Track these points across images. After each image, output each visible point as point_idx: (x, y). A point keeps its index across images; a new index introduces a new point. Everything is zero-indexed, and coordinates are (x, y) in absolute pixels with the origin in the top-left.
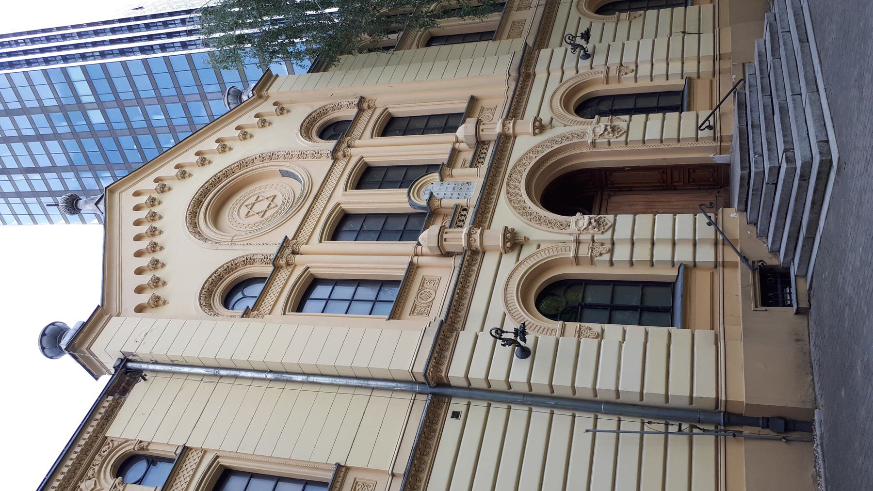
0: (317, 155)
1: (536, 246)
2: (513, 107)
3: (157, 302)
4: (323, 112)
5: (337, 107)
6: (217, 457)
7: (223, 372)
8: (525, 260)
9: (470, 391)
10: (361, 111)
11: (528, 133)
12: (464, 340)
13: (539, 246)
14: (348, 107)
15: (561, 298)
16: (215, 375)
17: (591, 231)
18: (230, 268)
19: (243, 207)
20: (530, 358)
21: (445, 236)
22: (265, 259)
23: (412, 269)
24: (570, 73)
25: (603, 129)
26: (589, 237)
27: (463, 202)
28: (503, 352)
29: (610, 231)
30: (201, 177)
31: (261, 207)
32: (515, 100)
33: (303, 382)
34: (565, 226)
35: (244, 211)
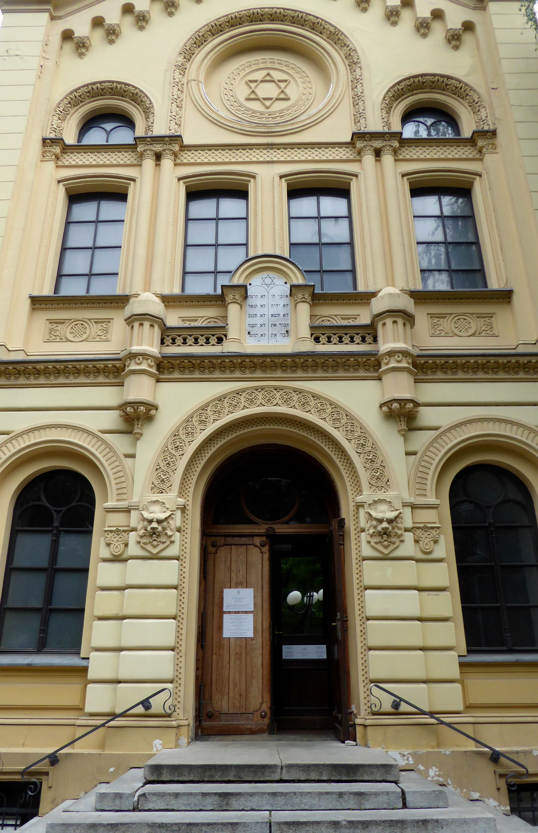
0: (358, 116)
1: (130, 451)
2: (501, 360)
4: (460, 90)
5: (475, 106)
18: (136, 97)
19: (265, 72)
22: (149, 128)
25: (380, 516)
26: (133, 524)
27: (232, 333)
34: (160, 485)
35: (259, 75)
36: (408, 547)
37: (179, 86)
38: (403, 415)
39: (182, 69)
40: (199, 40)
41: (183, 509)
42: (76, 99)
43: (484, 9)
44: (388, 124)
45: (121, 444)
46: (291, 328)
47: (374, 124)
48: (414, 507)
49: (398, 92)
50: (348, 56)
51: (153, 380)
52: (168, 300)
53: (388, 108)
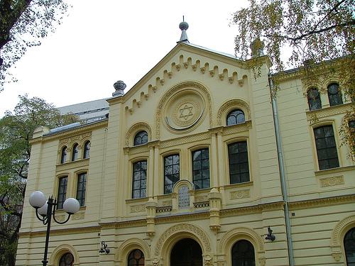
0: (211, 122)
4: (243, 104)
5: (248, 109)
12: (113, 231)
18: (147, 126)
24: (260, 232)
31: (186, 112)
35: (183, 107)
37: (158, 120)
38: (216, 230)
39: (159, 113)
40: (163, 101)
41: (162, 259)
42: (130, 131)
44: (220, 123)
48: (218, 256)
49: (222, 109)
52: (159, 197)
53: (219, 116)
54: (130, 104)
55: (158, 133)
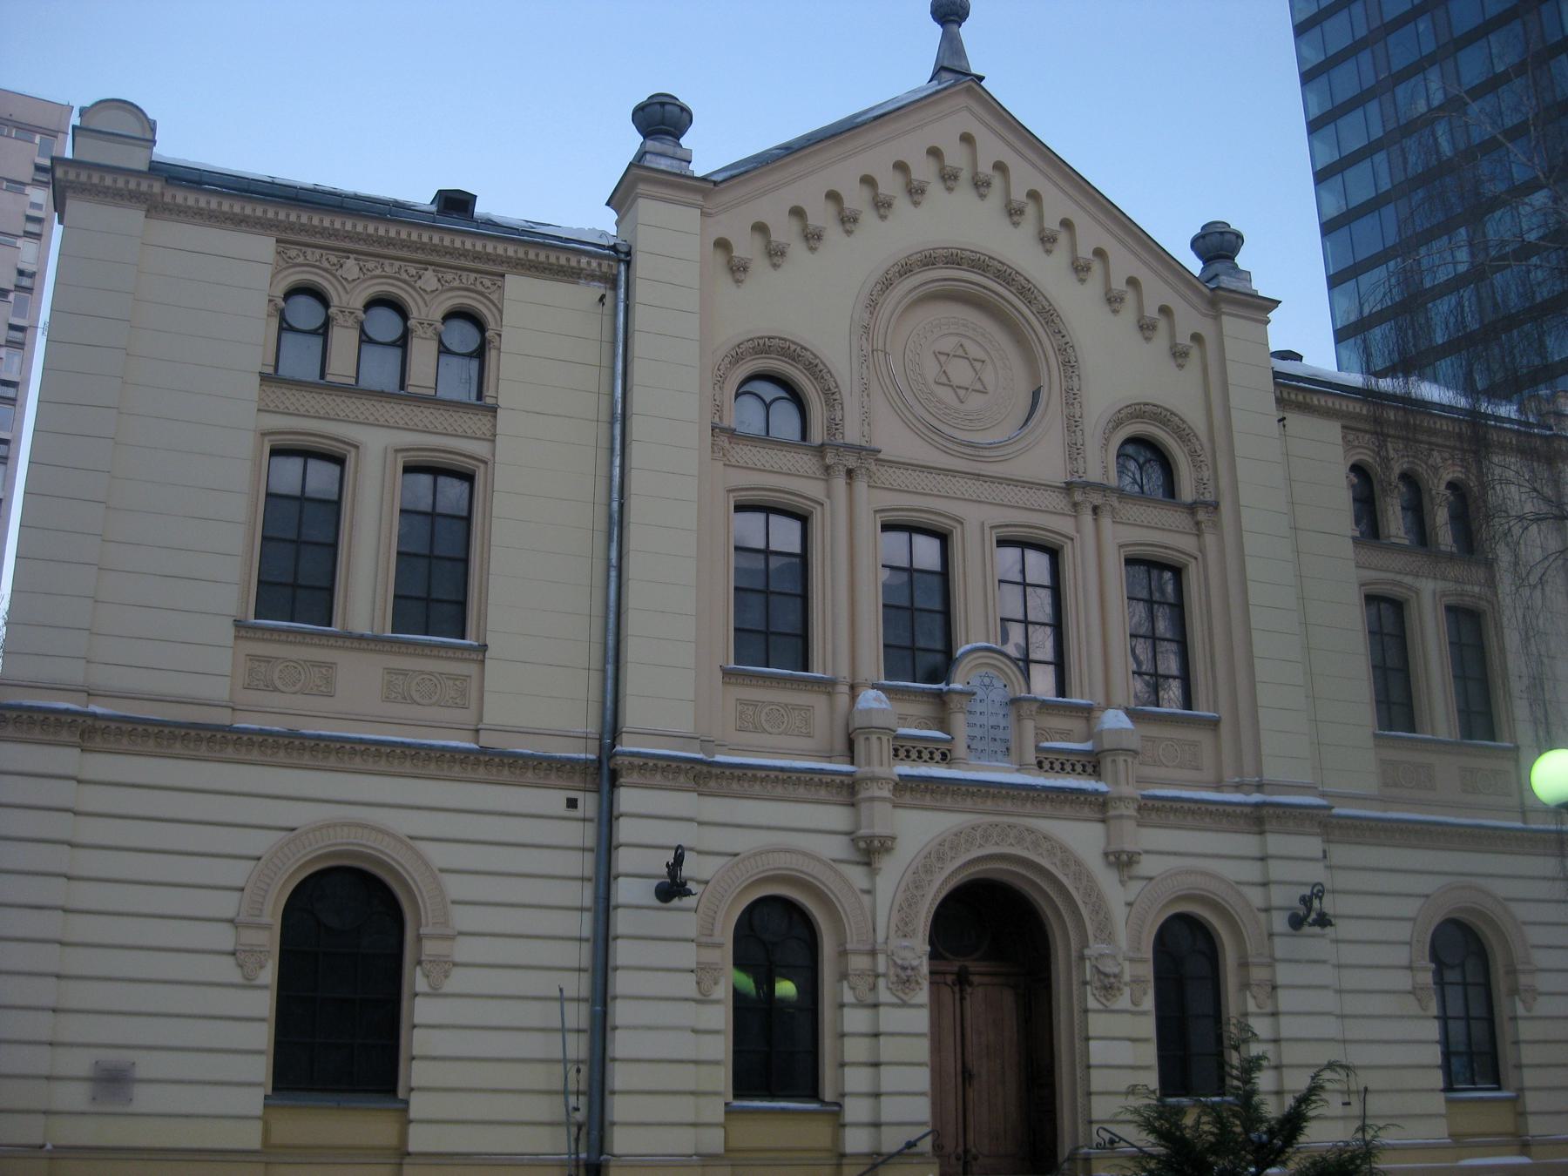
0: (1074, 451)
3: (737, 270)
4: (1183, 433)
6: (485, 463)
7: (618, 427)
8: (836, 872)
9: (608, 819)
10: (1192, 508)
11: (1108, 843)
13: (868, 892)
14: (1200, 481)
15: (777, 935)
16: (613, 414)
17: (892, 971)
18: (815, 369)
19: (954, 340)
20: (657, 903)
21: (874, 738)
22: (833, 426)
23: (826, 686)
28: (659, 863)
29: (895, 1000)
30: (1015, 247)
32: (1193, 806)
33: (609, 559)
35: (948, 344)
36: (1123, 1001)
38: (1122, 862)
43: (1217, 317)
45: (857, 876)
46: (1013, 745)
47: (1094, 475)
50: (1062, 350)
51: (889, 806)
54: (735, 226)
55: (866, 419)
